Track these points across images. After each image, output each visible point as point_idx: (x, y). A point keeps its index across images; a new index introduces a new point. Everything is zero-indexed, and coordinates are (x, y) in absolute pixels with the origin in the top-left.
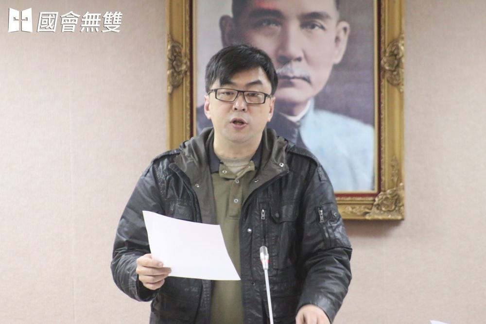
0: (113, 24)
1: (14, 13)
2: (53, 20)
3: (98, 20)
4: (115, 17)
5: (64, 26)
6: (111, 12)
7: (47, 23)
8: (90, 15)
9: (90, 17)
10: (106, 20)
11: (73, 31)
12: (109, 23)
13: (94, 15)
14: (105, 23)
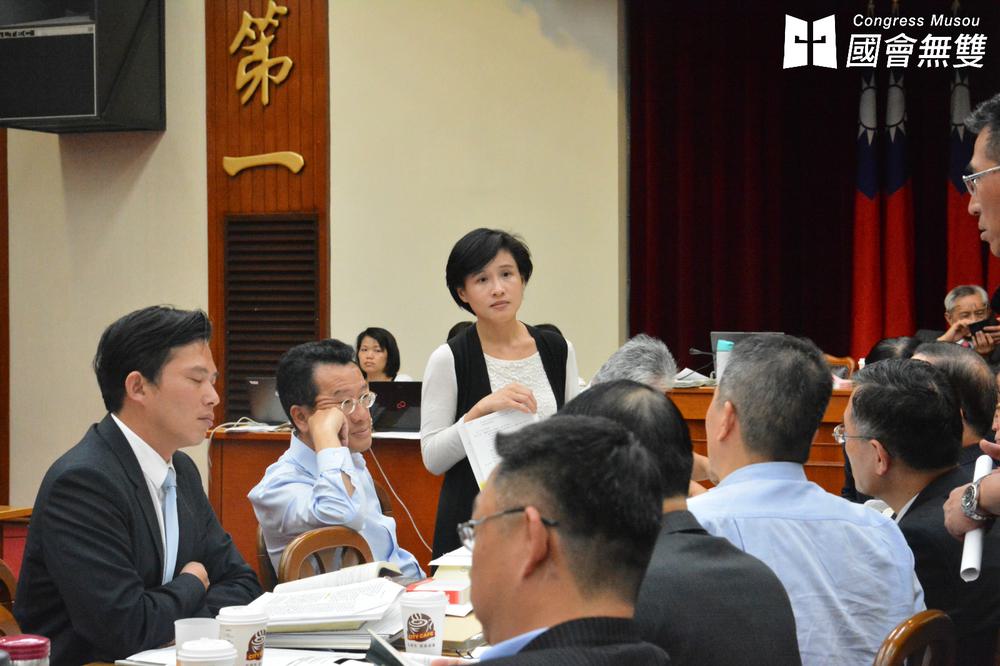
0: (970, 55)
1: (794, 26)
2: (873, 48)
3: (946, 47)
4: (974, 43)
5: (890, 58)
6: (968, 35)
7: (861, 53)
8: (934, 39)
9: (933, 43)
10: (959, 48)
11: (905, 65)
12: (964, 52)
13: (940, 39)
14: (958, 52)
